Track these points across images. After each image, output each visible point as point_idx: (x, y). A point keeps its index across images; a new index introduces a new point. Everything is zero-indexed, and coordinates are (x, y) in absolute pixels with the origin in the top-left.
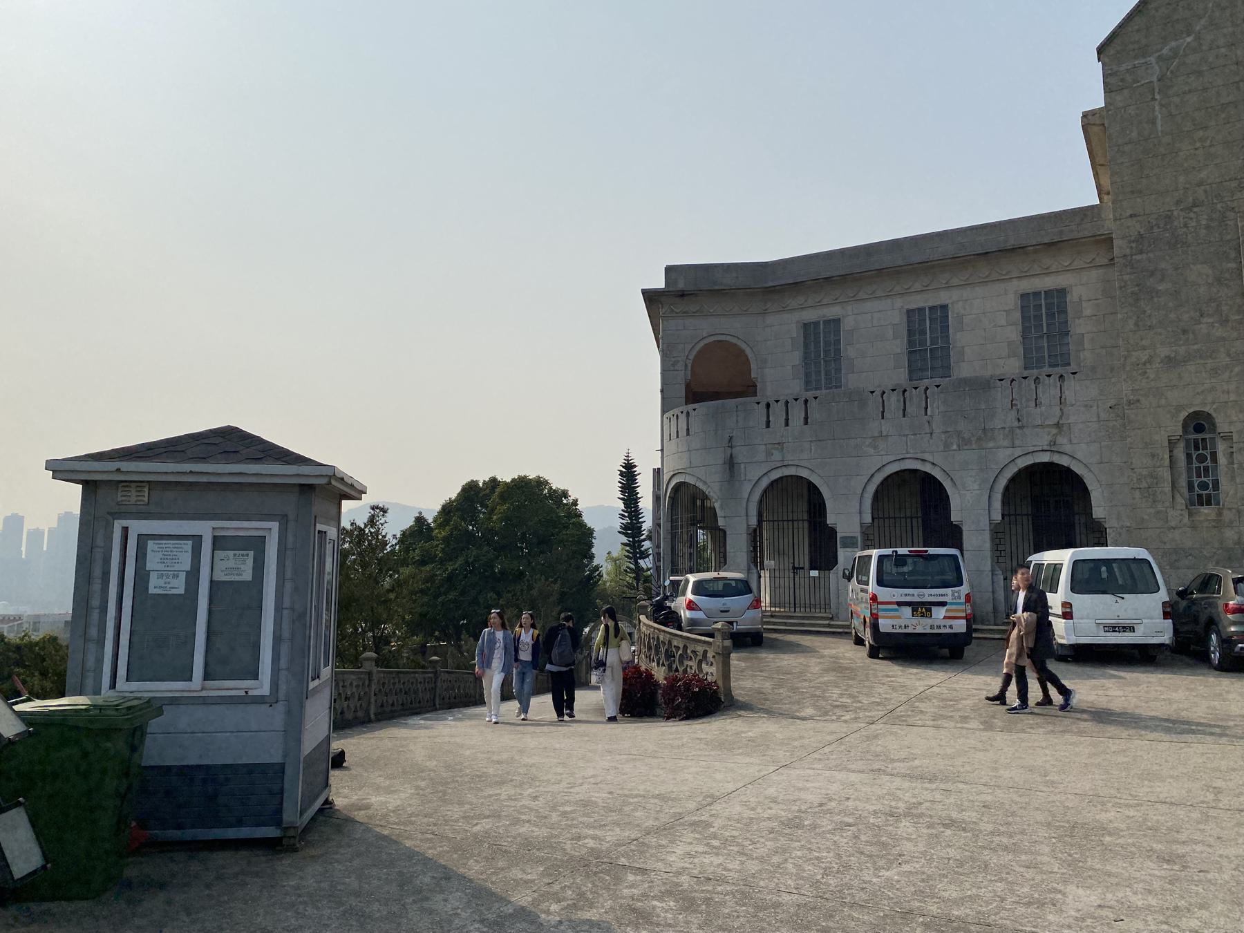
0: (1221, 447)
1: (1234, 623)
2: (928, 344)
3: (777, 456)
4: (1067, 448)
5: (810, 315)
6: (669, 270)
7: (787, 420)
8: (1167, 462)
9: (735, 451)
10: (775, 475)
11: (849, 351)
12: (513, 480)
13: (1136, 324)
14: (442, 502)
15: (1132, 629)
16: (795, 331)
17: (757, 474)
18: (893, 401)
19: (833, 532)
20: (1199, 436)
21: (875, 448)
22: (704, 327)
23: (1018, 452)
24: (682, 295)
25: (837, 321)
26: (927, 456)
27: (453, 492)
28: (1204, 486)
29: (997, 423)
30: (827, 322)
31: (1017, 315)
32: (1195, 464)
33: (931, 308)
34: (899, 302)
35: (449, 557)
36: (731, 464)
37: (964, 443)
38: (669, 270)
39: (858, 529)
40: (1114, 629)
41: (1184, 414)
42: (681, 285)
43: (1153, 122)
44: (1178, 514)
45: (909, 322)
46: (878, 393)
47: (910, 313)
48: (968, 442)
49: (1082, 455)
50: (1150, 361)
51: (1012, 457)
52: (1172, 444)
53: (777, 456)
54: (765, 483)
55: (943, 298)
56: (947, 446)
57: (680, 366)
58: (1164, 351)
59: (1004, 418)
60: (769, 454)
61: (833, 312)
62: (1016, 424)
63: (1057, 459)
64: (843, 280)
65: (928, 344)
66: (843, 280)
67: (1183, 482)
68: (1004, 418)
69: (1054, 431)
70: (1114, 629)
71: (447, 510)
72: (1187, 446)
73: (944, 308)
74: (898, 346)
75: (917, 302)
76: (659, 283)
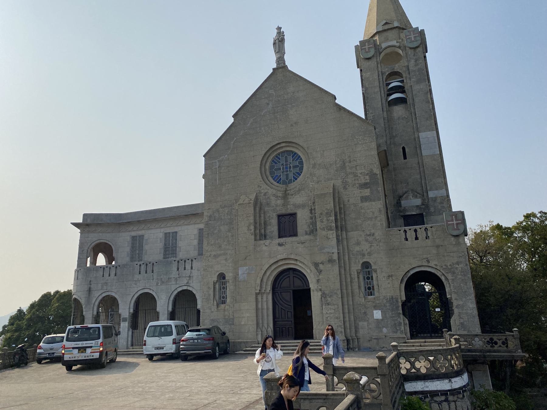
0: (228, 284)
1: (182, 345)
2: (170, 247)
3: (105, 287)
4: (191, 285)
5: (133, 234)
6: (85, 215)
7: (110, 274)
8: (212, 290)
9: (92, 286)
10: (104, 295)
11: (146, 247)
12: (64, 292)
13: (208, 244)
14: (31, 303)
15: (163, 348)
16: (129, 239)
17: (97, 295)
18: (143, 267)
19: (120, 315)
20: (224, 281)
21: (136, 284)
22: (96, 237)
23: (178, 286)
24: (88, 225)
25: (143, 236)
26: (151, 288)
27: (36, 298)
28: (223, 297)
29: (172, 276)
30: (140, 236)
31: (197, 236)
32: (222, 290)
33: (173, 233)
34: (162, 230)
35: (29, 326)
36: (90, 290)
37: (163, 282)
38: (85, 215)
39: (128, 314)
40: (157, 348)
41: (218, 273)
42: (89, 221)
43: (216, 180)
44: (214, 308)
45: (166, 237)
46: (139, 265)
47: (166, 234)
48: (163, 282)
49: (196, 288)
50: (210, 256)
51: (175, 288)
52: (215, 284)
53: (105, 287)
54: (100, 298)
55: (176, 229)
56: (157, 284)
57: (85, 251)
58: (214, 253)
59: (174, 273)
60: (102, 286)
61: (140, 233)
62: (178, 276)
63: (189, 288)
64: (145, 222)
65: (170, 247)
66: (145, 222)
67: (217, 297)
68: (174, 273)
69: (188, 279)
70: (157, 348)
71: (32, 306)
72: (220, 285)
73: (176, 232)
74: (161, 245)
75: (168, 230)
76: (80, 220)
